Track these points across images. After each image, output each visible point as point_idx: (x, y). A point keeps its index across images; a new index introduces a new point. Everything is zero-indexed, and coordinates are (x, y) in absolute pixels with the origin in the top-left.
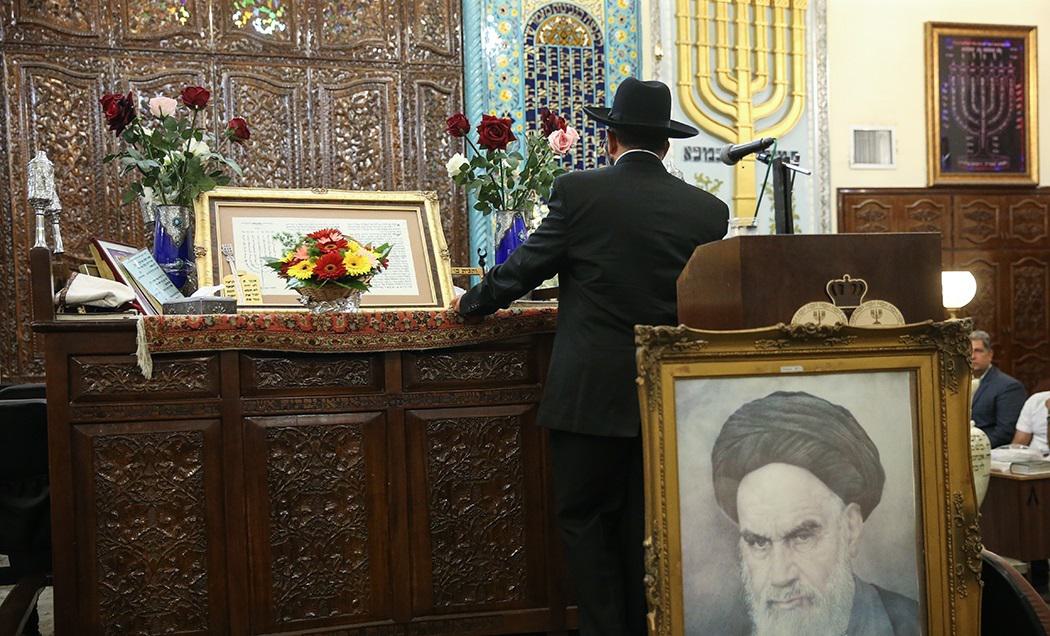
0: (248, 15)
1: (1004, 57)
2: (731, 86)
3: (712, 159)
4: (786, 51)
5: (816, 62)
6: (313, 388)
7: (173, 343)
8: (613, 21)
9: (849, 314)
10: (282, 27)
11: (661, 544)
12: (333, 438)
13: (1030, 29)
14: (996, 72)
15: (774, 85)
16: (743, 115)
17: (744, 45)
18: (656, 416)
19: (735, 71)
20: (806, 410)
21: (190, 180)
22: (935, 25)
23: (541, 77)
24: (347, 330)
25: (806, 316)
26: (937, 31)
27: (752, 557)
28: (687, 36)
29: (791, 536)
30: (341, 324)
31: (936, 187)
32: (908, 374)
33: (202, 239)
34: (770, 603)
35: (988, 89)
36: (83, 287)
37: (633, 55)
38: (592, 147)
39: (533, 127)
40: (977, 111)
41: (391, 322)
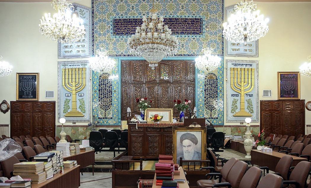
0: (163, 77)
1: (294, 77)
2: (240, 84)
3: (236, 96)
6: (153, 131)
7: (140, 126)
8: (219, 75)
10: (168, 79)
11: (174, 146)
12: (156, 136)
14: (292, 80)
15: (248, 84)
16: (242, 89)
17: (243, 77)
18: (174, 135)
20: (190, 135)
21: (144, 108)
22: (279, 72)
23: (207, 84)
24: (157, 125)
25: (190, 126)
27: (184, 148)
28: (232, 76)
29: (188, 146)
30: (156, 124)
32: (201, 132)
33: (145, 114)
34: (185, 152)
36: (133, 120)
37: (222, 80)
38: (215, 95)
39: (205, 92)
40: (288, 87)
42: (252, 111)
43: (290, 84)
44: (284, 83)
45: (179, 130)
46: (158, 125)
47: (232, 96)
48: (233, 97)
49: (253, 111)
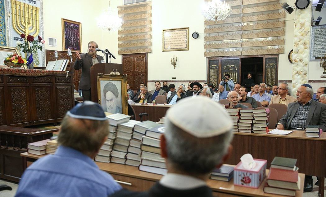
1: (76, 28)
4: (35, 19)
5: (41, 23)
9: (115, 73)
13: (80, 23)
17: (27, 16)
19: (25, 22)
22: (64, 19)
24: (24, 72)
26: (64, 21)
27: (107, 102)
29: (110, 100)
31: (64, 51)
34: (109, 108)
35: (73, 33)
37: (3, 14)
41: (49, 72)
42: (38, 63)
43: (73, 35)
44: (68, 34)
45: (102, 79)
46: (19, 71)
47: (15, 39)
48: (15, 41)
49: (39, 62)
